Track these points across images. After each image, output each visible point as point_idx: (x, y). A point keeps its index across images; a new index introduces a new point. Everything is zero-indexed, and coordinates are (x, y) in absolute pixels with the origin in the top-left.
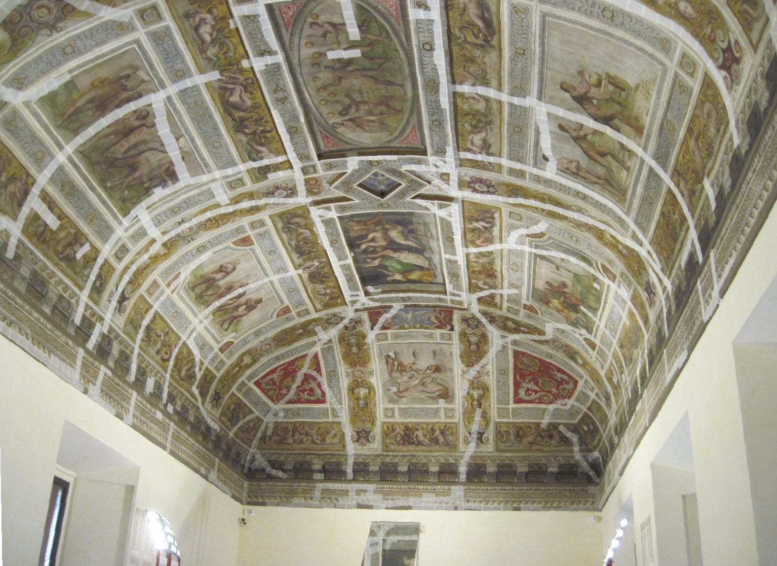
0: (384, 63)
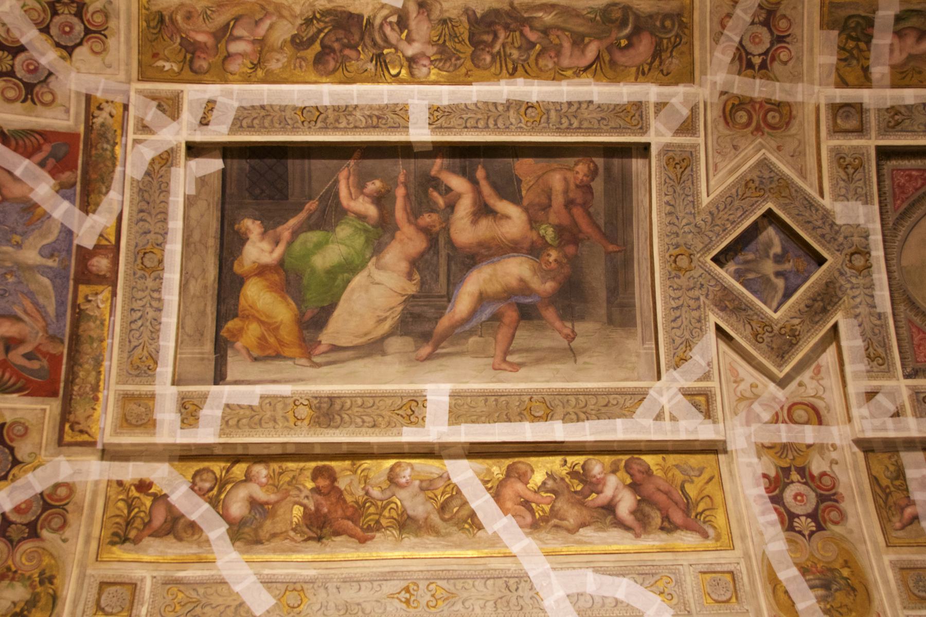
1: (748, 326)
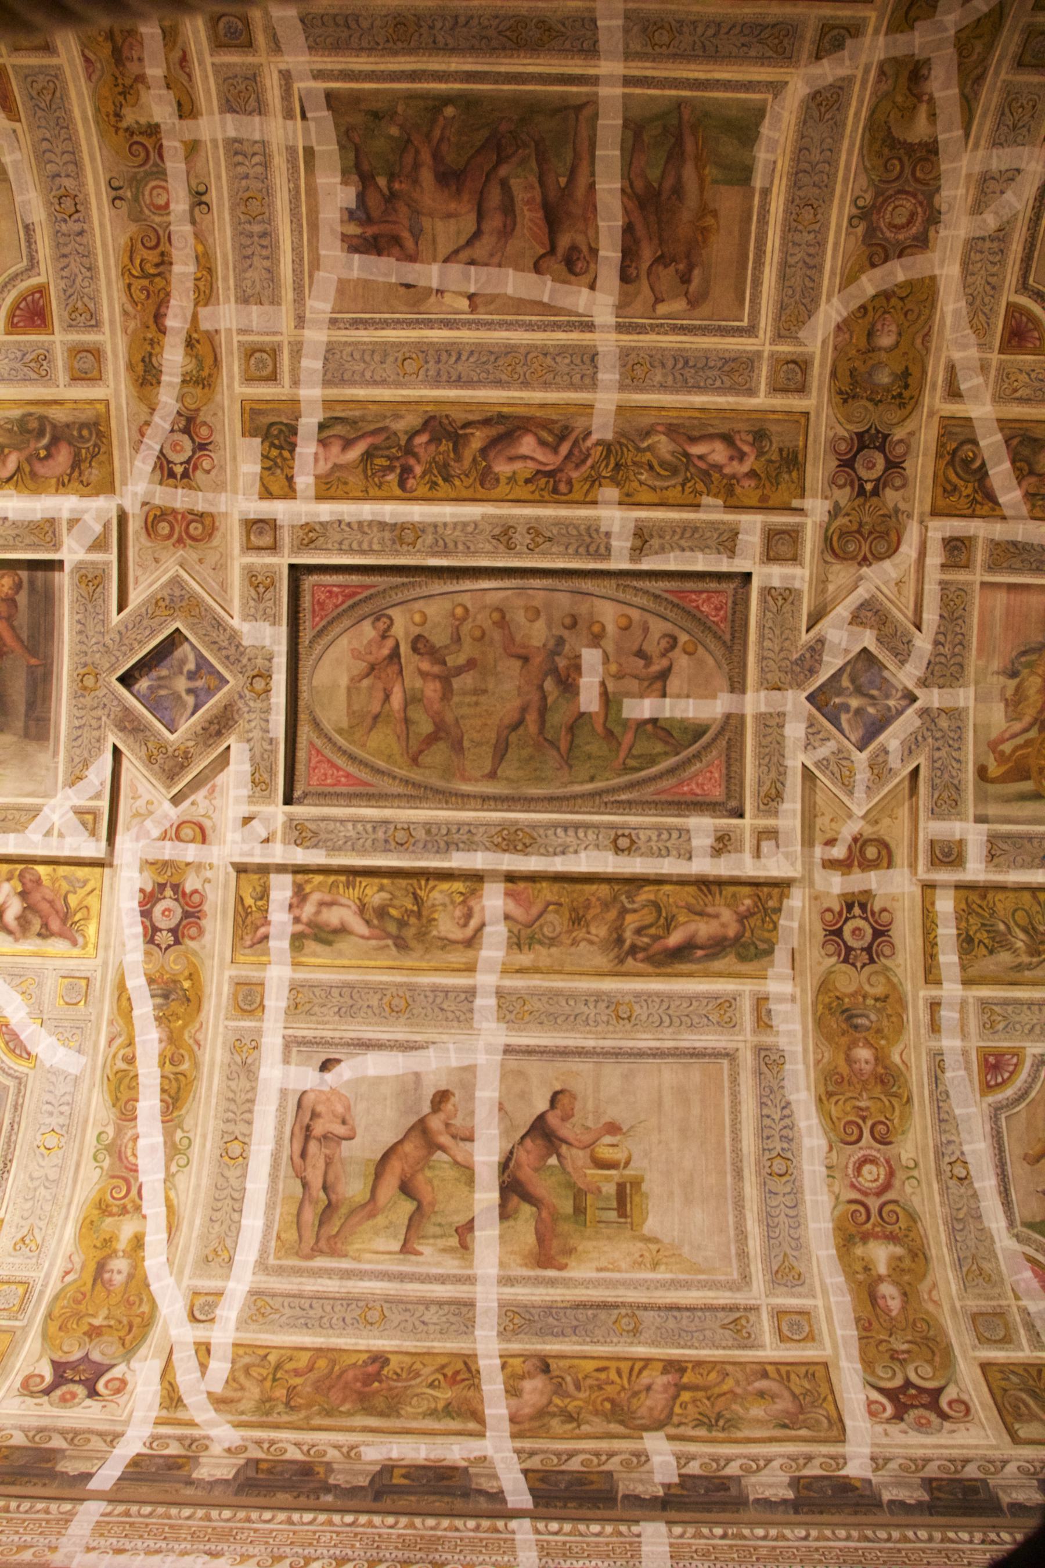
0: (558, 749)
1: (144, 748)
